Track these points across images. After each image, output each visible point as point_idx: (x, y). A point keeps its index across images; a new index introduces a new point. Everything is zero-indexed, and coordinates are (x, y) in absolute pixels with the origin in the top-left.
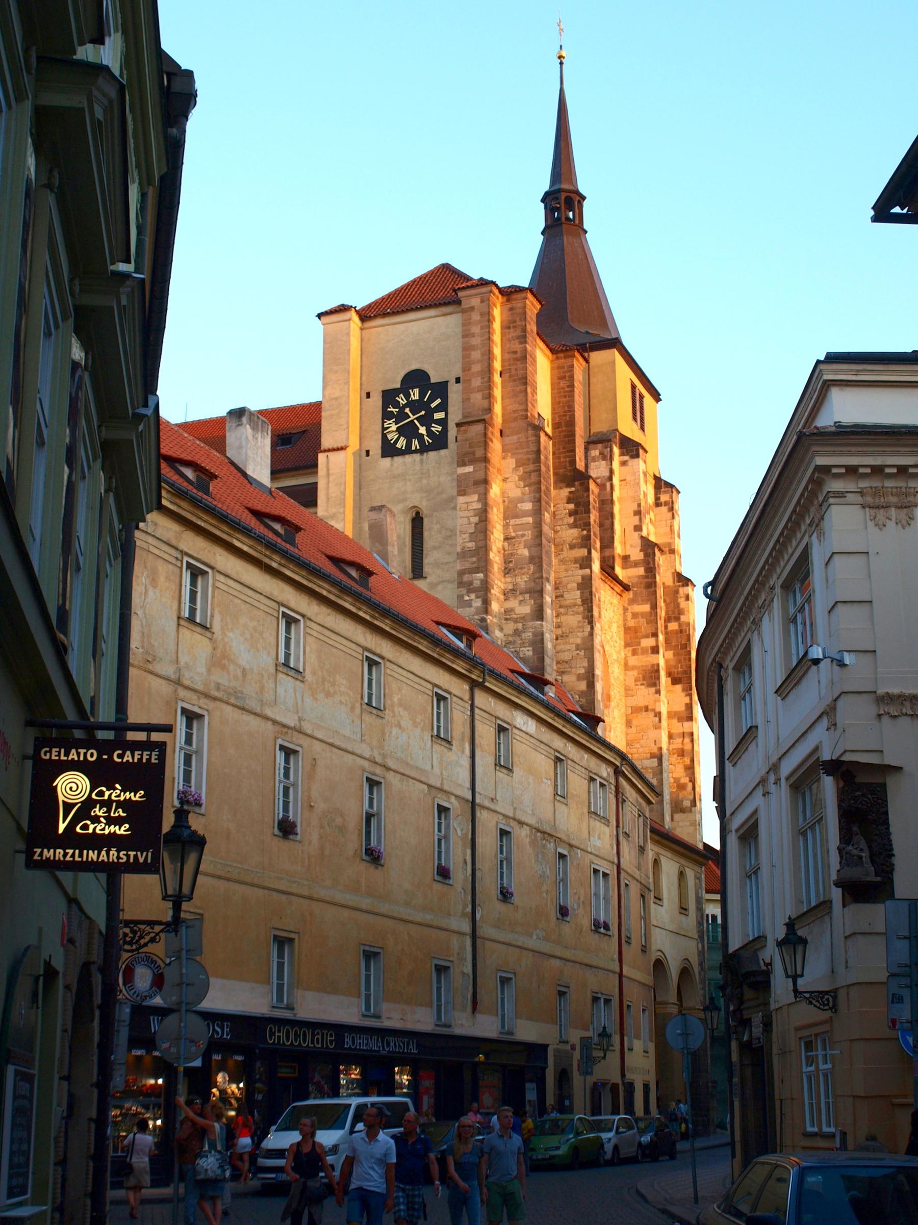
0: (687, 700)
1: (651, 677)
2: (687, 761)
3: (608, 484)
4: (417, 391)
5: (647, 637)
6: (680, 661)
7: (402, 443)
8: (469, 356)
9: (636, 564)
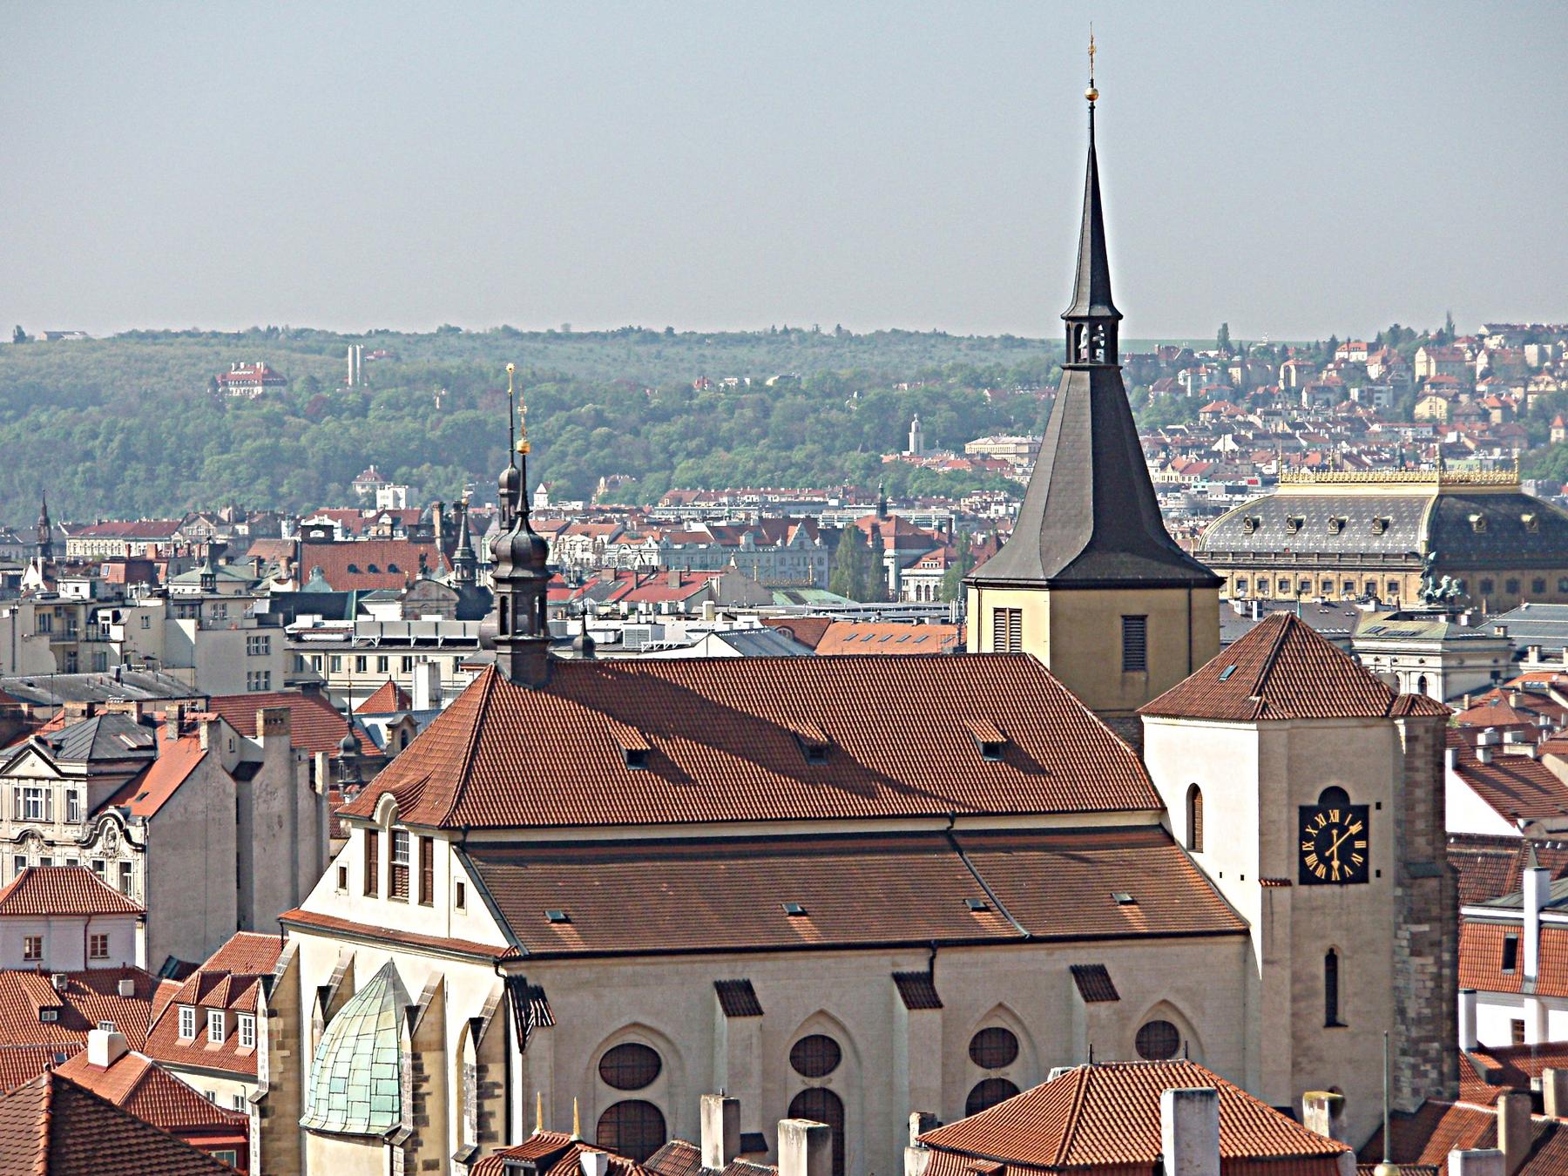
4: (1337, 812)
7: (1321, 872)
8: (1411, 793)
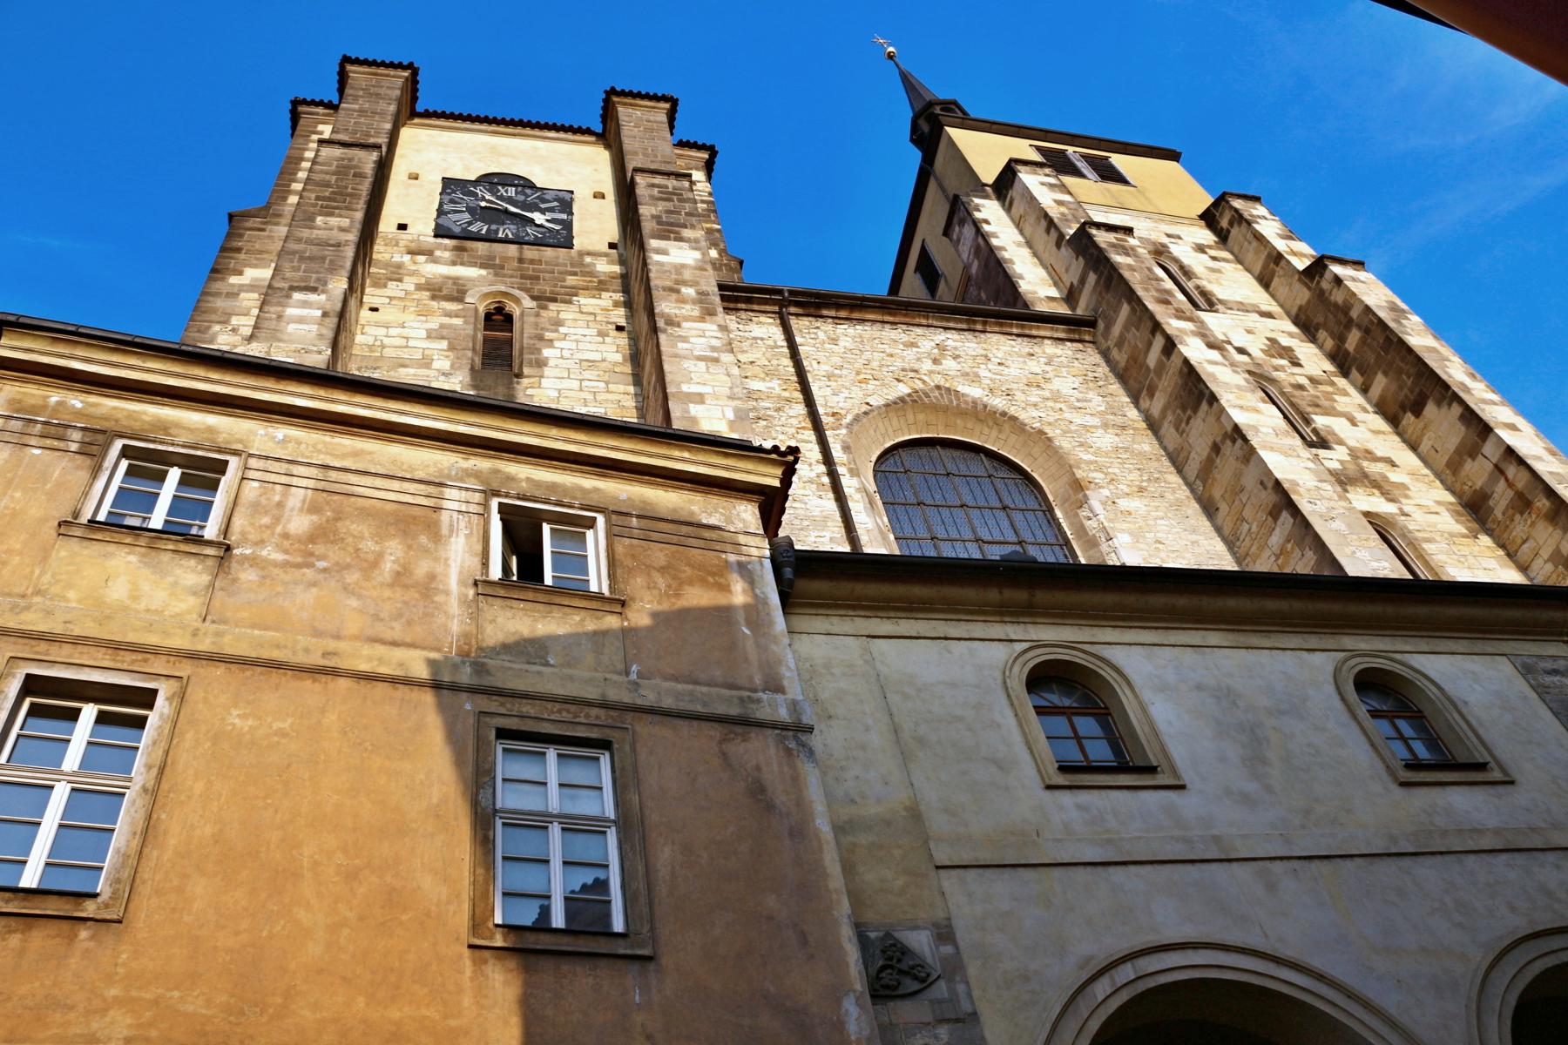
0: (1456, 410)
1: (1190, 392)
2: (1543, 503)
3: (980, 240)
5: (1149, 344)
6: (1400, 372)
9: (1083, 281)
